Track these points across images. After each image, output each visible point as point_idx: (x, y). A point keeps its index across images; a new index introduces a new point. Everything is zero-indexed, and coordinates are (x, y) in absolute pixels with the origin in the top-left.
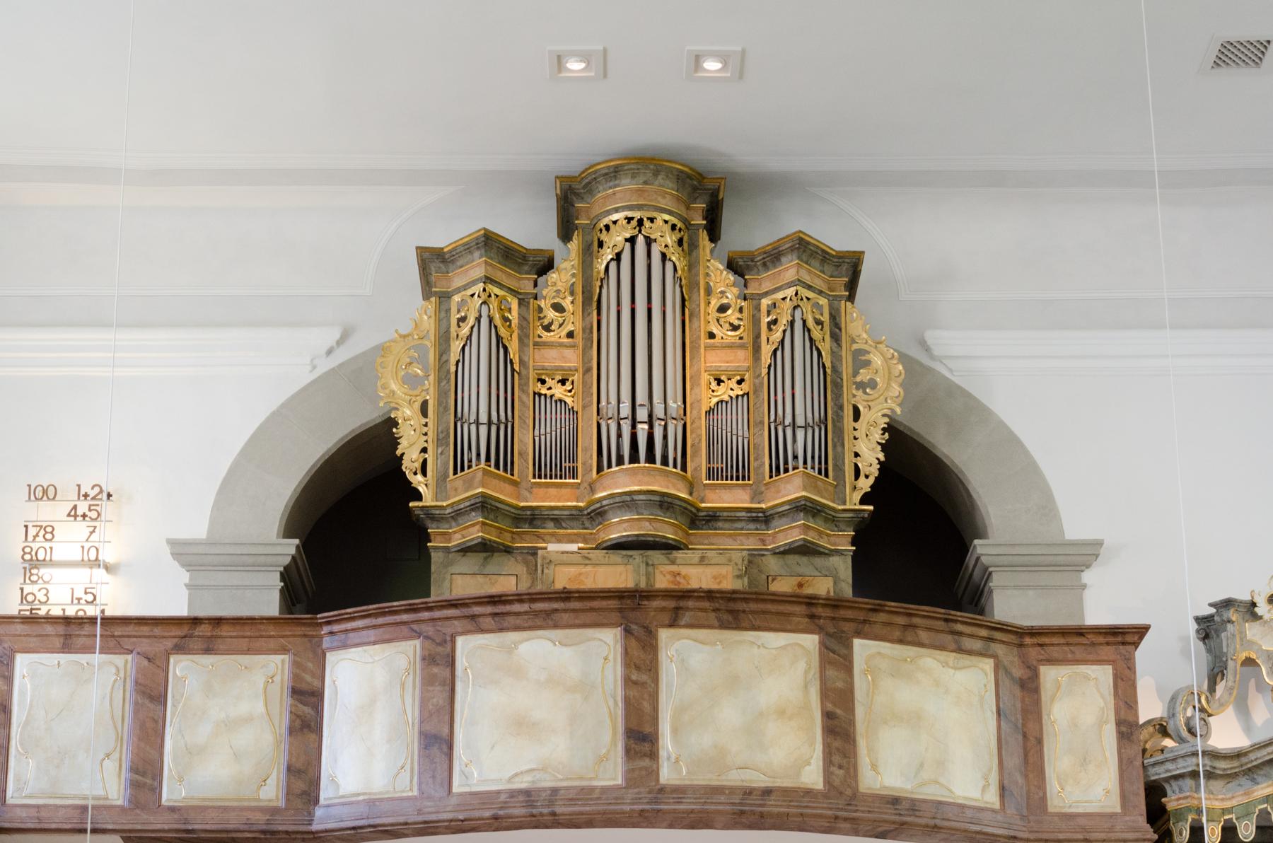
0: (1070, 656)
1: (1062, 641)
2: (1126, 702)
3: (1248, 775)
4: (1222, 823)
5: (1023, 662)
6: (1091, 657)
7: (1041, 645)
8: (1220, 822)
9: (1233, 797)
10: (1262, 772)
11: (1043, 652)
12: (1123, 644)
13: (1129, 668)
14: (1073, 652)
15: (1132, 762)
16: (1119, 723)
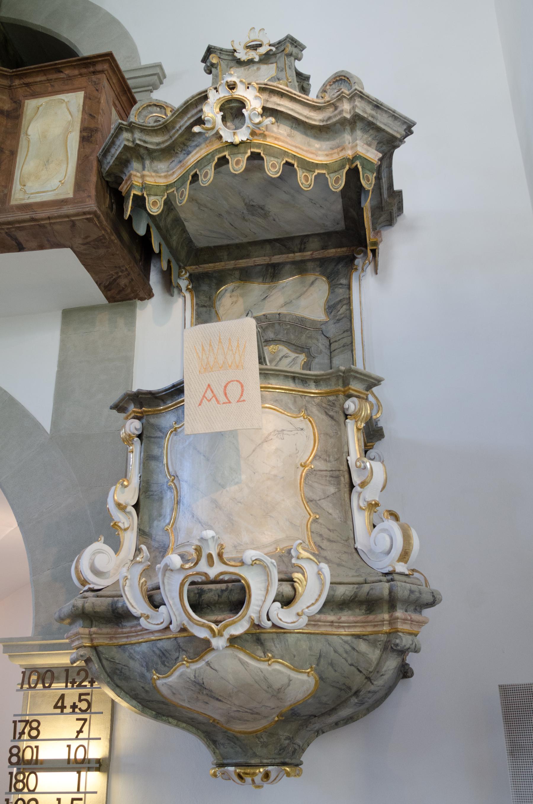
0: (50, 89)
1: (44, 78)
2: (90, 115)
3: (184, 150)
4: (166, 197)
5: (11, 99)
6: (66, 87)
7: (27, 85)
8: (163, 196)
9: (174, 172)
10: (194, 144)
11: (28, 90)
12: (94, 73)
13: (97, 90)
14: (52, 86)
15: (88, 157)
16: (83, 130)
